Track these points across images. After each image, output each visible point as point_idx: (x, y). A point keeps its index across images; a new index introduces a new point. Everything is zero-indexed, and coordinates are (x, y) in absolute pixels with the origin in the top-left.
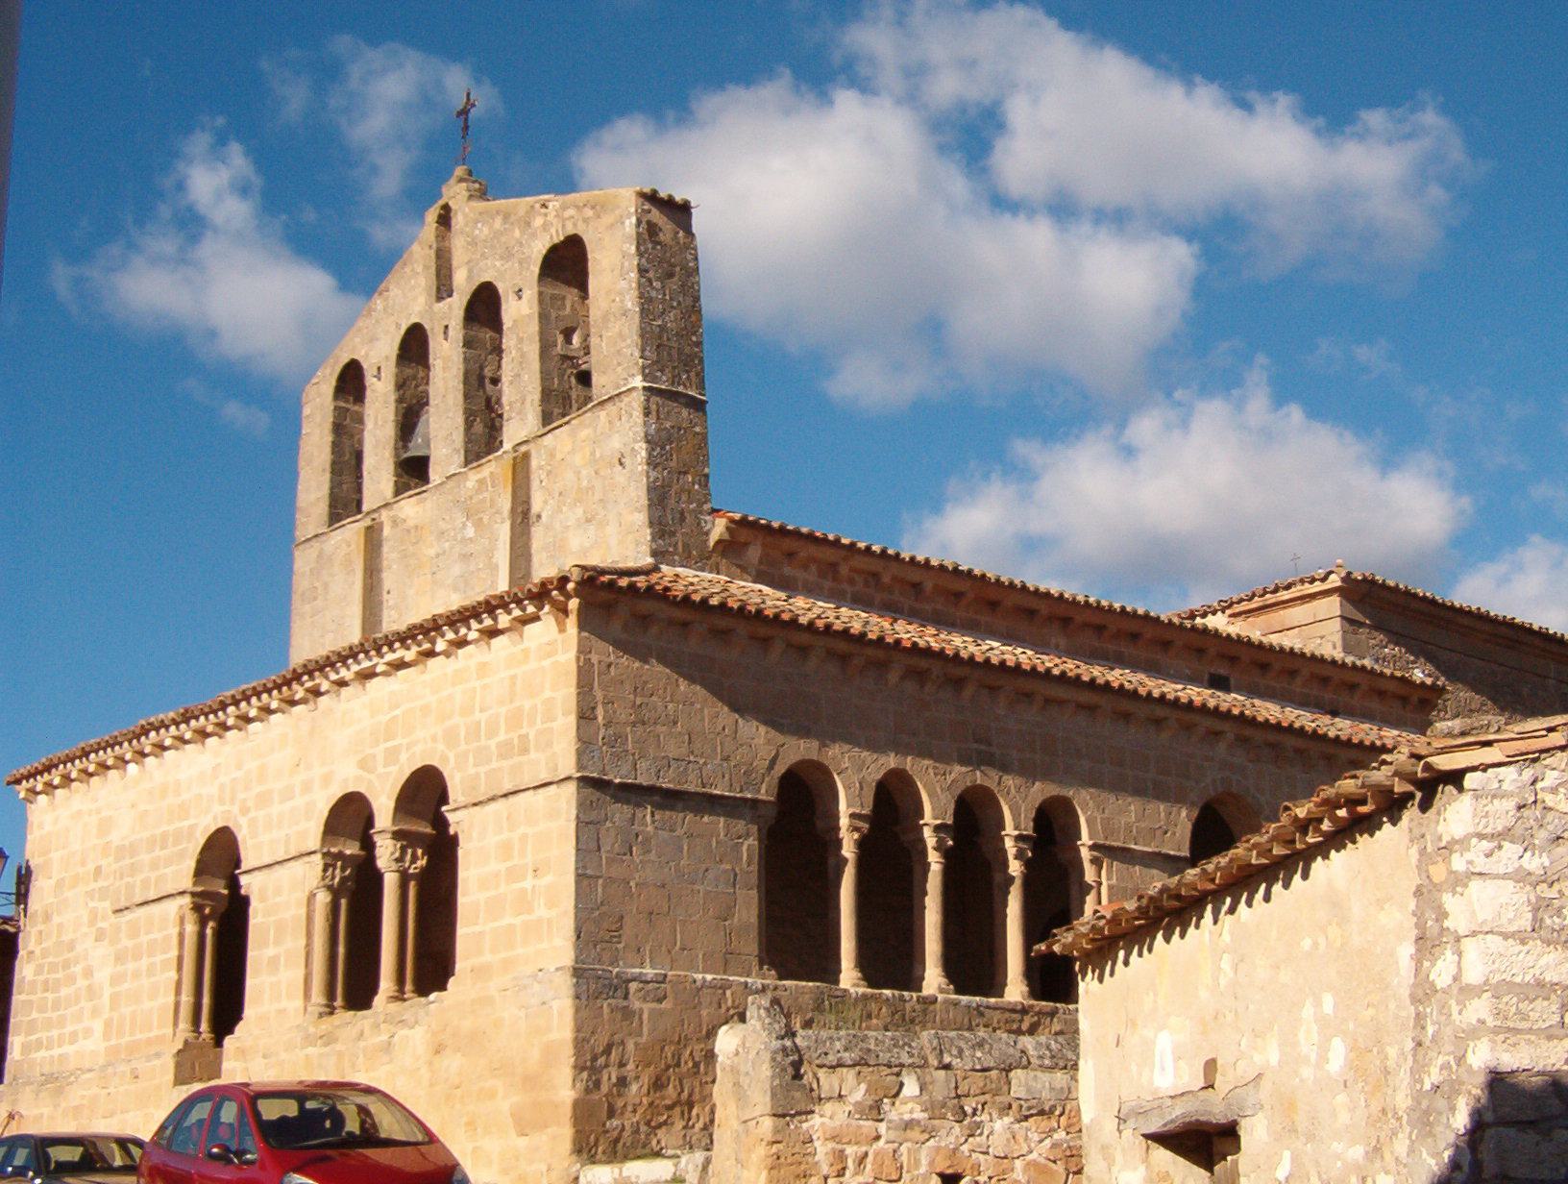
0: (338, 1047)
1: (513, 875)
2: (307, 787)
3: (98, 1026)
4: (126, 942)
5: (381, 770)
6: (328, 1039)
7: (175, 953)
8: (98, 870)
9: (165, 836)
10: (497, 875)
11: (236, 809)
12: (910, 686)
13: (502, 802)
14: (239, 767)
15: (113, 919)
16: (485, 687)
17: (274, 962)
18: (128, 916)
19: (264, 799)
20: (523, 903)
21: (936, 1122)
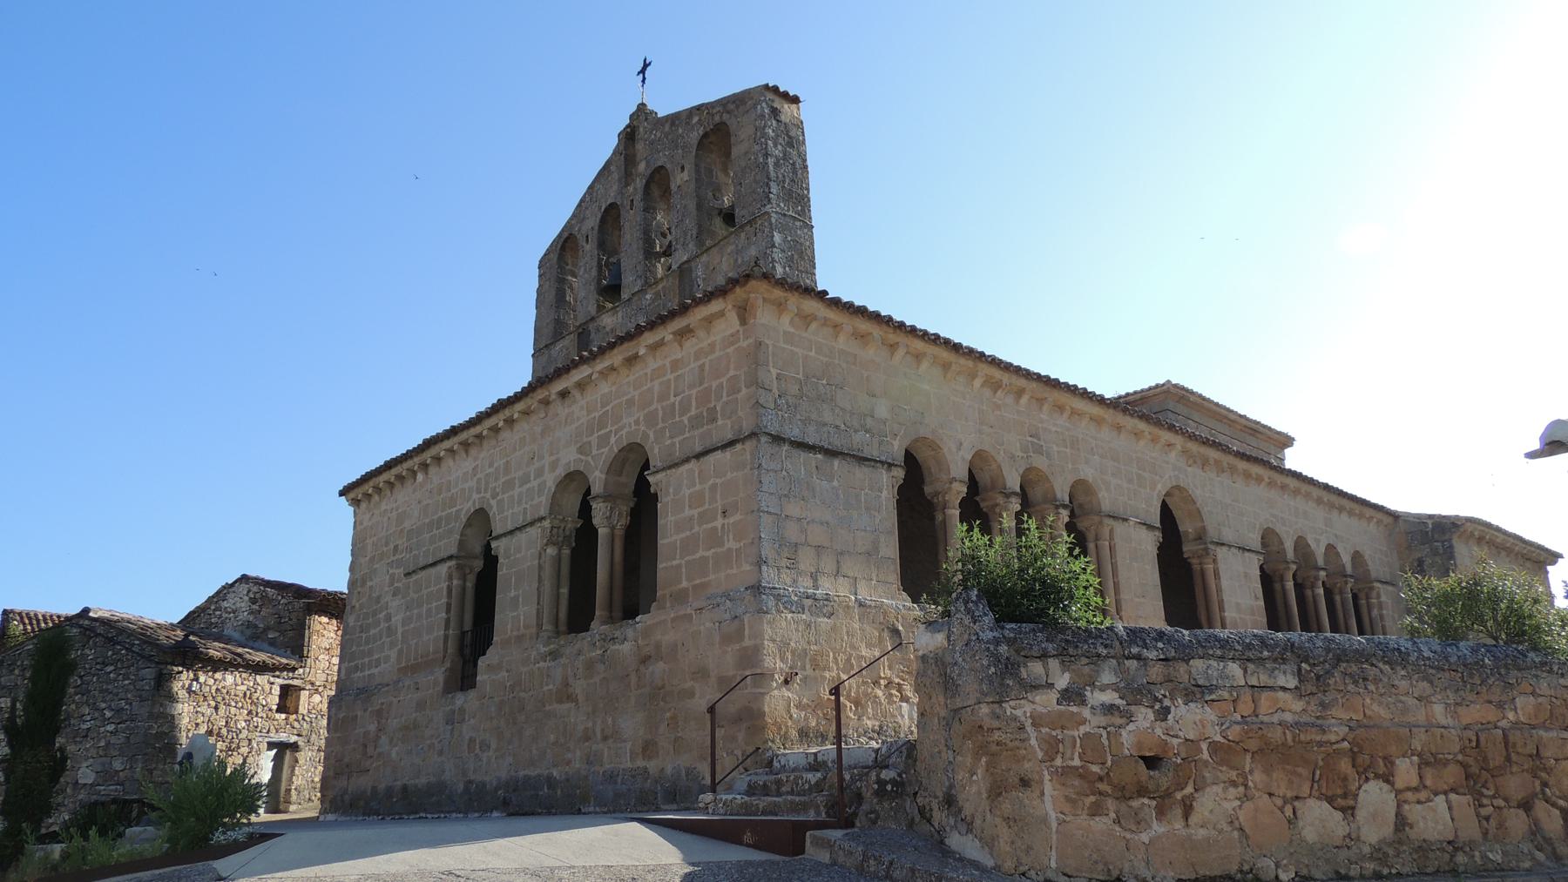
0: (563, 660)
1: (703, 518)
2: (540, 472)
3: (393, 654)
4: (413, 595)
5: (594, 452)
6: (554, 655)
7: (444, 600)
8: (396, 547)
9: (440, 519)
10: (691, 518)
11: (488, 495)
12: (987, 392)
13: (693, 464)
14: (491, 465)
15: (404, 580)
16: (677, 378)
17: (515, 602)
18: (415, 577)
19: (509, 485)
20: (715, 539)
21: (1133, 708)
